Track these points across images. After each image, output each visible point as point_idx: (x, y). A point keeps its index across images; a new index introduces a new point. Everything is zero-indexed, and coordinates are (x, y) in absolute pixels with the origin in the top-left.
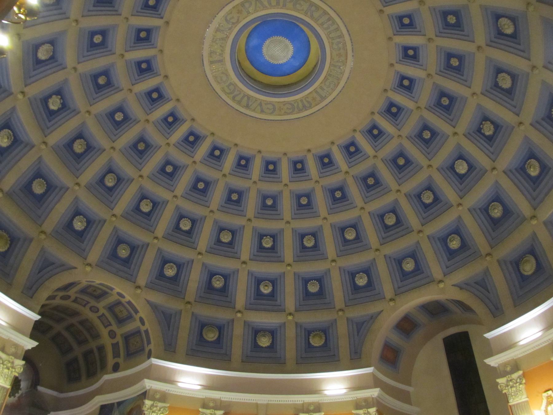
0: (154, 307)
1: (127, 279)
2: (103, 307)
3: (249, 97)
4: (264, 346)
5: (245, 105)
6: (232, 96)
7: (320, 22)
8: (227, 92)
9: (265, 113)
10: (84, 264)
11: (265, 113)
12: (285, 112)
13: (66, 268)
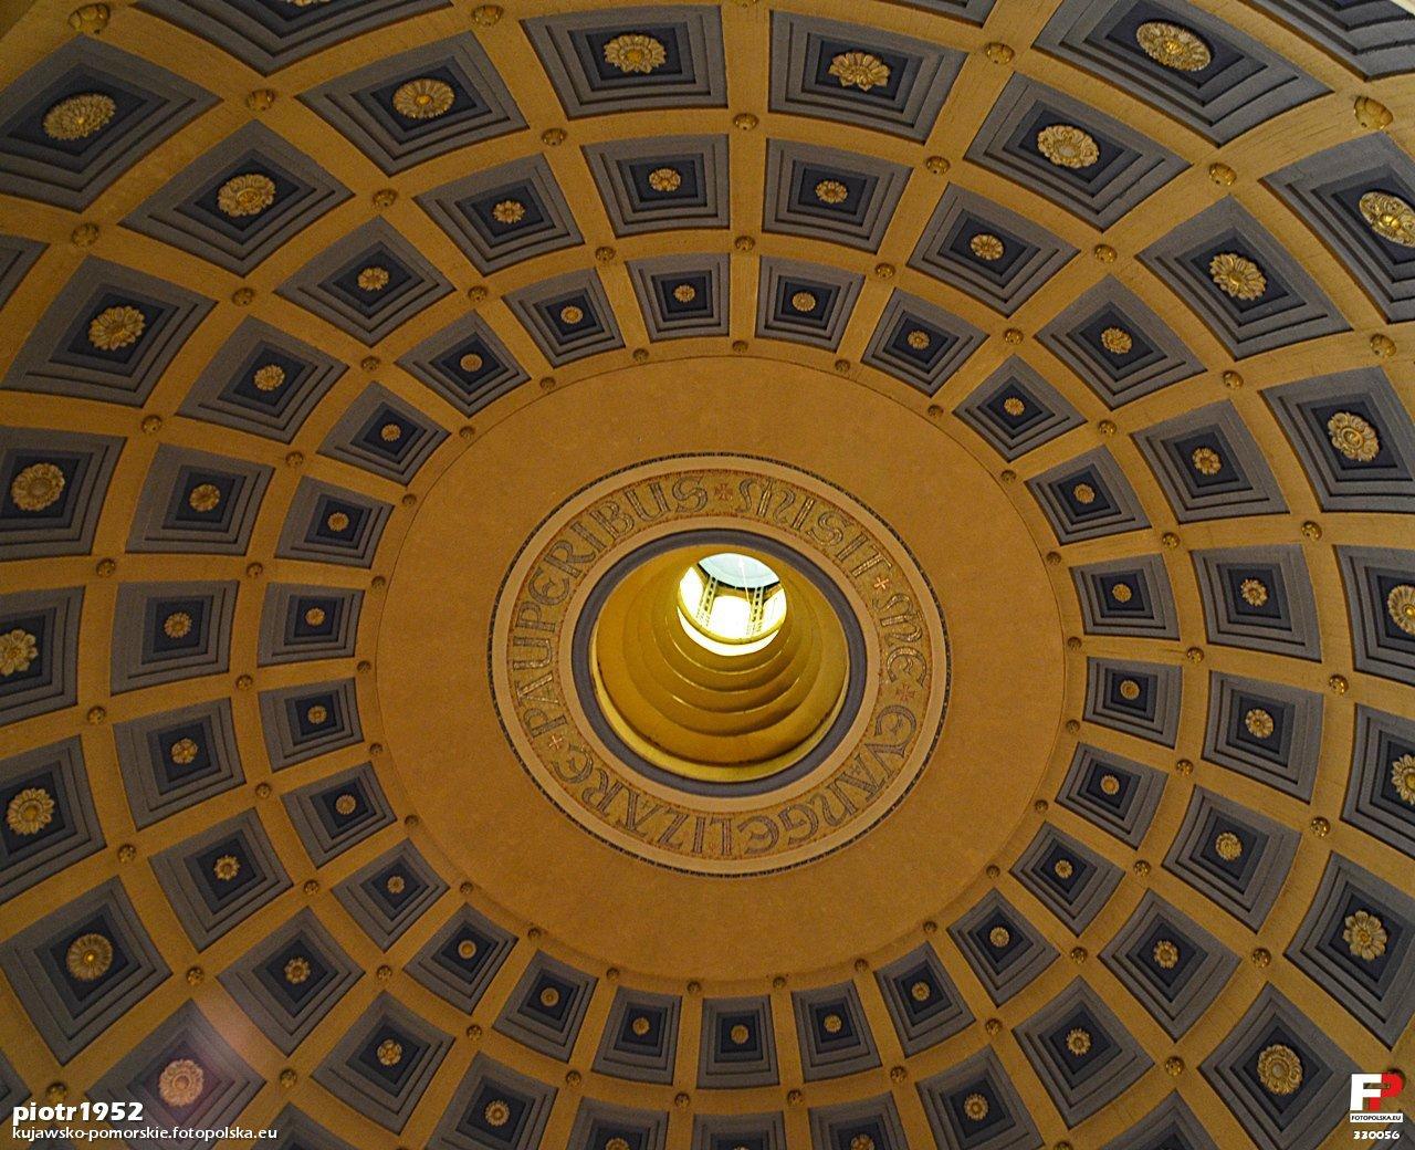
3: (840, 776)
5: (867, 794)
6: (823, 824)
7: (606, 539)
8: (807, 832)
9: (906, 743)
11: (906, 743)
12: (920, 681)
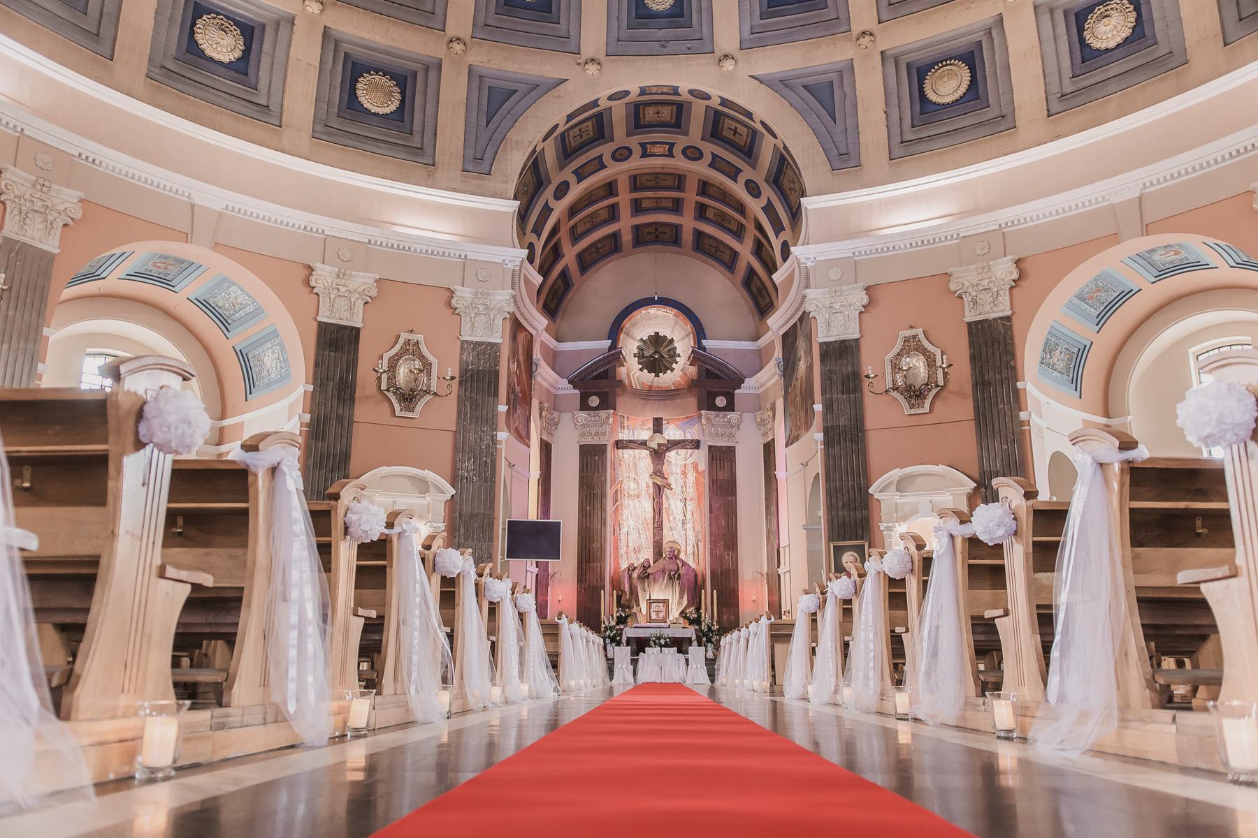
0: (781, 85)
1: (690, 52)
2: (629, 134)
4: (1112, 44)
10: (579, 64)
13: (539, 89)
